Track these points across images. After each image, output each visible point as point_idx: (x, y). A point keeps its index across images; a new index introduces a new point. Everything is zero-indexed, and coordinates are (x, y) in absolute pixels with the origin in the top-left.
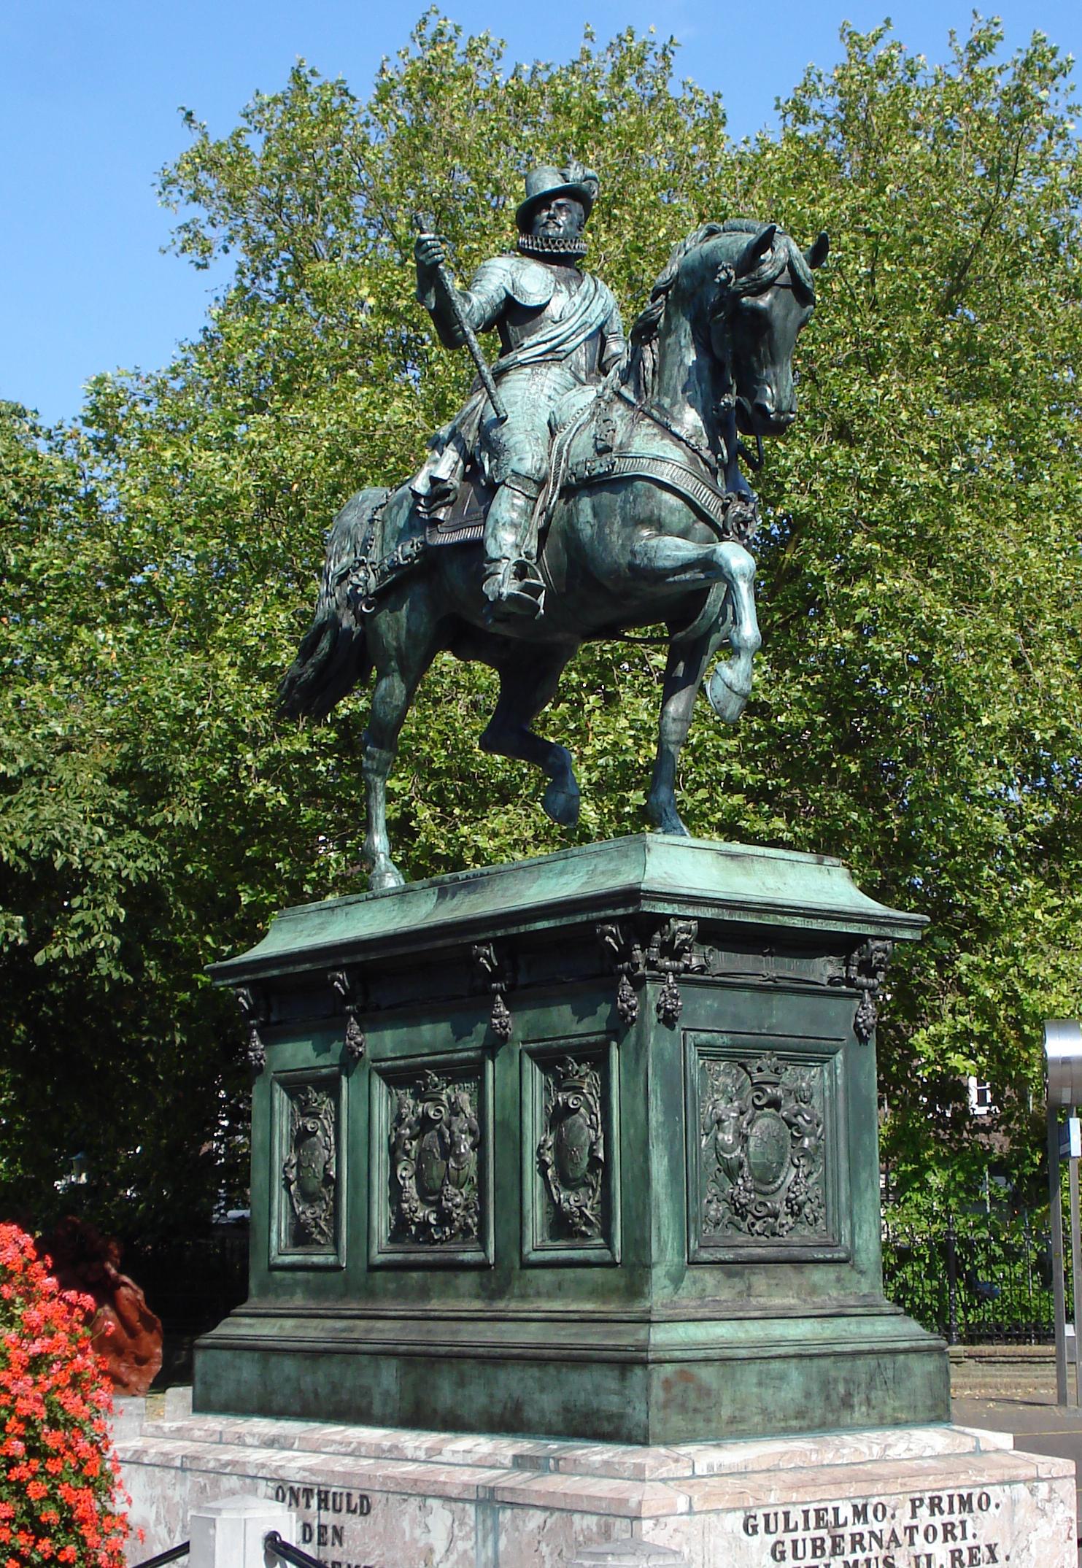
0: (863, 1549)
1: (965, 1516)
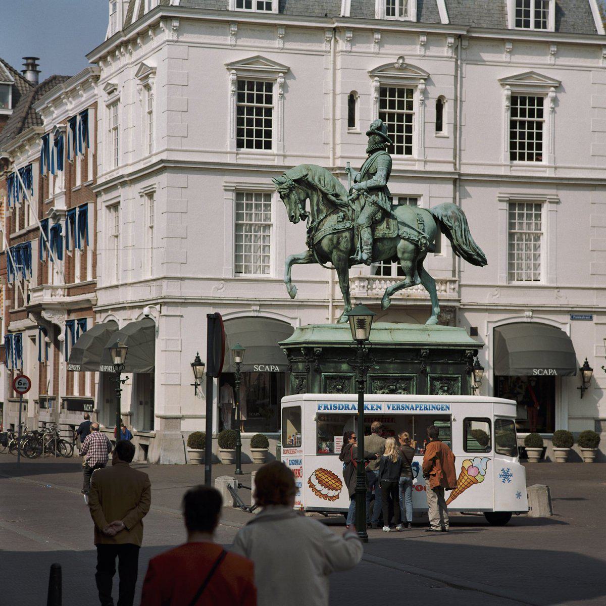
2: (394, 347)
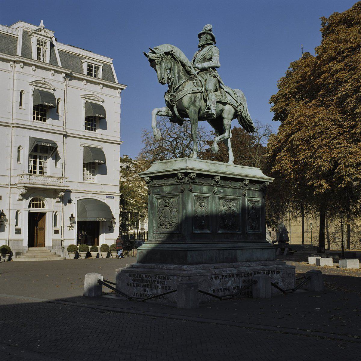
0: (147, 283)
1: (164, 280)
2: (233, 176)
